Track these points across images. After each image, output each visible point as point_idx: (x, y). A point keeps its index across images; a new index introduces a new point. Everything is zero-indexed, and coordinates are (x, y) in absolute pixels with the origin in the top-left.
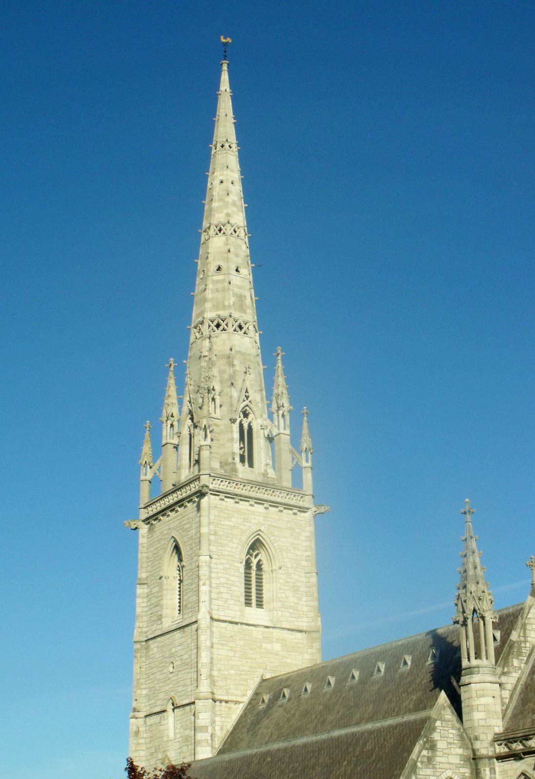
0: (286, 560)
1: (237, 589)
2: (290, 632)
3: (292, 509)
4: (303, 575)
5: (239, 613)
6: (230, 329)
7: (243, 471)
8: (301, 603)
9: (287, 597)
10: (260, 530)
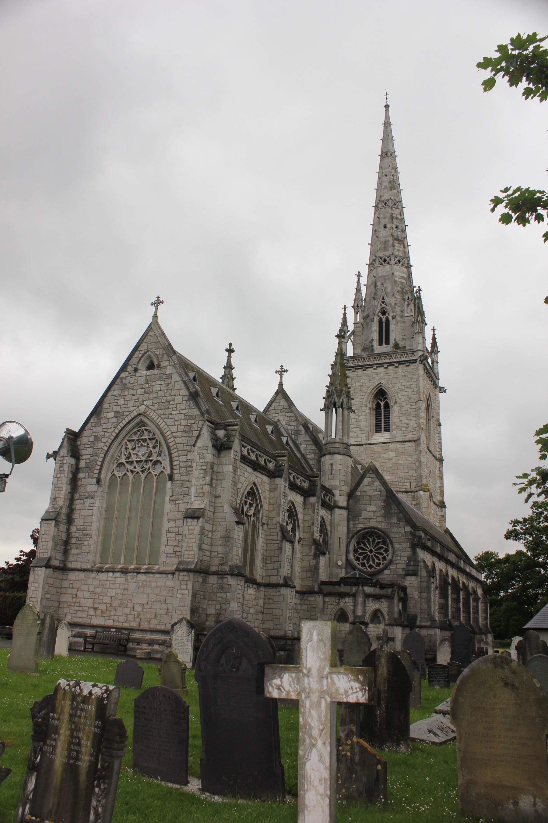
0: (400, 397)
1: (363, 423)
2: (402, 443)
3: (405, 364)
4: (414, 404)
5: (365, 438)
6: (393, 262)
7: (378, 349)
9: (401, 421)
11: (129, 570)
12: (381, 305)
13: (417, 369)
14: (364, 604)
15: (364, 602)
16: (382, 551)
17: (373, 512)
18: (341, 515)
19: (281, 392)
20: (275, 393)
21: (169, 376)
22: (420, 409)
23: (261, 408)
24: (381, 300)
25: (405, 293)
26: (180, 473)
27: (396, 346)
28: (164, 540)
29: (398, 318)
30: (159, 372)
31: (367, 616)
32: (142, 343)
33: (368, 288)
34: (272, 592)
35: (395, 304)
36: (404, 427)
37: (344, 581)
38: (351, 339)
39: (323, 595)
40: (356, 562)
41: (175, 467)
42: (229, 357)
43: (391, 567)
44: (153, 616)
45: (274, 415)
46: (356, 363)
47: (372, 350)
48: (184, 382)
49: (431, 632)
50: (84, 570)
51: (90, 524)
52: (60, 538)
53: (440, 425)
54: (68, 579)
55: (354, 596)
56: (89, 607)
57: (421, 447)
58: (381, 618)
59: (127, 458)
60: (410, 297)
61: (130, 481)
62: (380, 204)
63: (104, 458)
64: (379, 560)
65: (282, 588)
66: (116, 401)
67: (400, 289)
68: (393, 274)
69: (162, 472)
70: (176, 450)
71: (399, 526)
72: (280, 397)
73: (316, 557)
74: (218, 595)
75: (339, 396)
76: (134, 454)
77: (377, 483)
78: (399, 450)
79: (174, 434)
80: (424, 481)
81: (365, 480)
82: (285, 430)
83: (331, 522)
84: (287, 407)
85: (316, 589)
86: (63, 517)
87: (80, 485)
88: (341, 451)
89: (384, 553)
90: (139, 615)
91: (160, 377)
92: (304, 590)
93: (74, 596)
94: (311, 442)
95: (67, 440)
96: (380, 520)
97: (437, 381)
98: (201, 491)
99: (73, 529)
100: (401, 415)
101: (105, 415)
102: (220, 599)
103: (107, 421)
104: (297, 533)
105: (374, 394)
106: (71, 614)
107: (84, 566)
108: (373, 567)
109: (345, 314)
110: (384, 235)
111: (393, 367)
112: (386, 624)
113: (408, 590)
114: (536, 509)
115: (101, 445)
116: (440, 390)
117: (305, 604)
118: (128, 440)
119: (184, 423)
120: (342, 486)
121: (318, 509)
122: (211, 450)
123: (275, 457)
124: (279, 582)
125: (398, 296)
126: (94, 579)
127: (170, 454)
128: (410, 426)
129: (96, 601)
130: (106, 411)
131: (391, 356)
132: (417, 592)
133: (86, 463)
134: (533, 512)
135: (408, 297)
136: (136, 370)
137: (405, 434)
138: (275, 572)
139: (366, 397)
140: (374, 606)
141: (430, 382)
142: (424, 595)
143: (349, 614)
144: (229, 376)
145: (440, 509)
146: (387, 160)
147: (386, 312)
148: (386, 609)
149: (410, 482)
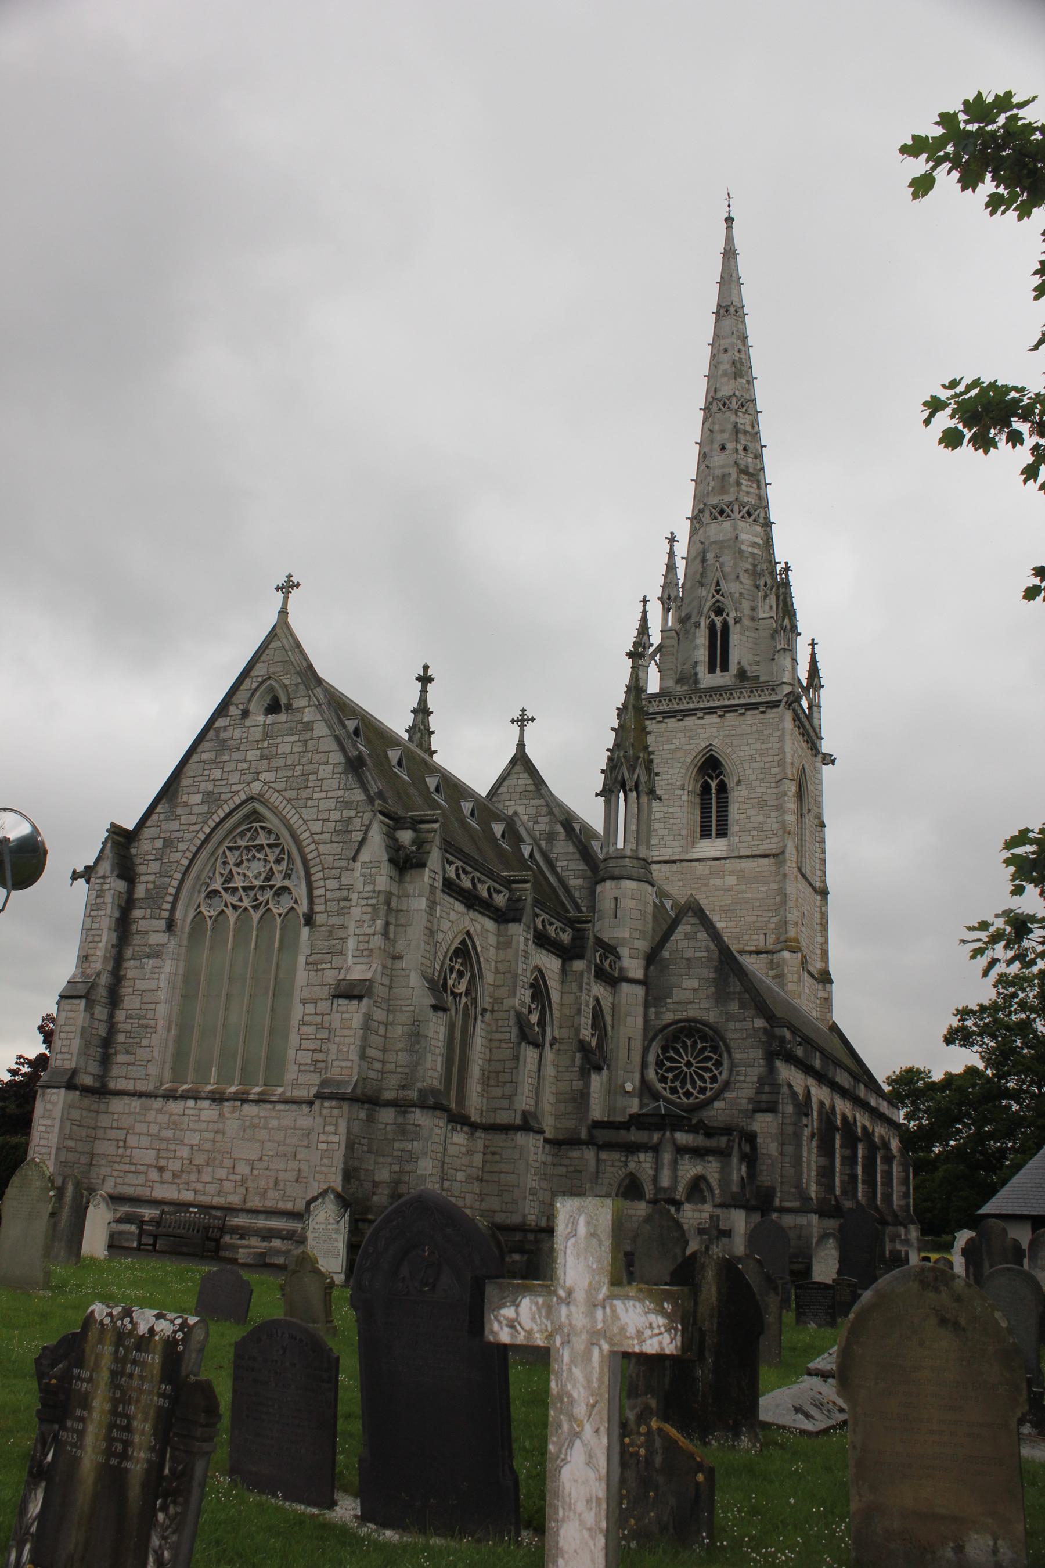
0: (747, 772)
2: (751, 860)
3: (757, 708)
4: (773, 785)
5: (680, 849)
6: (737, 515)
7: (707, 680)
8: (769, 820)
9: (748, 818)
10: (711, 745)
11: (226, 1096)
12: (714, 596)
13: (781, 719)
14: (675, 1163)
15: (675, 1163)
16: (709, 1064)
17: (694, 990)
18: (632, 995)
19: (521, 761)
20: (510, 762)
21: (308, 726)
22: (785, 795)
23: (483, 792)
24: (713, 588)
25: (760, 574)
26: (326, 911)
27: (742, 675)
28: (294, 1039)
29: (746, 622)
30: (290, 718)
31: (680, 1189)
32: (257, 661)
33: (689, 564)
34: (499, 1139)
35: (741, 594)
36: (755, 829)
37: (636, 1121)
38: (655, 661)
39: (595, 1147)
40: (659, 1086)
41: (316, 900)
42: (424, 691)
43: (727, 1095)
44: (271, 1185)
45: (507, 803)
46: (664, 707)
47: (696, 681)
48: (337, 738)
49: (802, 1220)
50: (141, 1095)
51: (153, 1006)
52: (94, 1032)
53: (822, 825)
54: (110, 1111)
55: (655, 1149)
56: (149, 1166)
57: (786, 868)
58: (706, 1194)
59: (226, 881)
60: (769, 582)
61: (231, 926)
62: (714, 404)
63: (182, 882)
64: (705, 1082)
65: (519, 1134)
66: (206, 772)
67: (749, 567)
68: (737, 538)
69: (292, 908)
70: (320, 867)
71: (742, 1017)
72: (518, 768)
73: (584, 1074)
74: (397, 1145)
75: (632, 769)
76: (239, 874)
77: (702, 935)
78: (744, 872)
79: (316, 837)
80: (792, 933)
81: (680, 928)
82: (528, 833)
83: (613, 1009)
84: (531, 788)
85: (584, 1135)
86: (101, 993)
87: (134, 931)
88: (634, 872)
89: (713, 1068)
90: (243, 1182)
91: (291, 729)
92: (561, 1137)
93: (121, 1144)
94: (577, 856)
95: (112, 847)
96: (707, 1006)
97: (818, 742)
98: (366, 946)
99: (120, 1016)
100: (750, 806)
101: (185, 798)
102: (400, 1153)
103: (187, 810)
104: (548, 1030)
105: (699, 764)
106: (113, 1179)
107: (141, 1087)
108: (692, 1094)
109: (644, 612)
110: (721, 463)
111: (736, 714)
112: (718, 1204)
113: (759, 1140)
114: (1004, 988)
115: (176, 856)
116: (824, 759)
117: (561, 1165)
118: (229, 848)
119: (335, 815)
120: (636, 941)
121: (588, 984)
122: (385, 868)
123: (508, 883)
124: (511, 1122)
125: (746, 579)
126: (159, 1111)
127: (308, 875)
128: (766, 827)
129: (163, 1154)
130: (186, 790)
131: (731, 694)
132: (775, 1144)
133: (147, 890)
134: (999, 994)
135: (766, 583)
136: (245, 714)
137: (757, 843)
138: (505, 1103)
139: (684, 771)
140: (694, 1169)
141: (804, 745)
142: (789, 1149)
143: (645, 1185)
144: (422, 727)
145: (820, 987)
146: (727, 323)
147: (723, 610)
148: (716, 1175)
149: (765, 934)
